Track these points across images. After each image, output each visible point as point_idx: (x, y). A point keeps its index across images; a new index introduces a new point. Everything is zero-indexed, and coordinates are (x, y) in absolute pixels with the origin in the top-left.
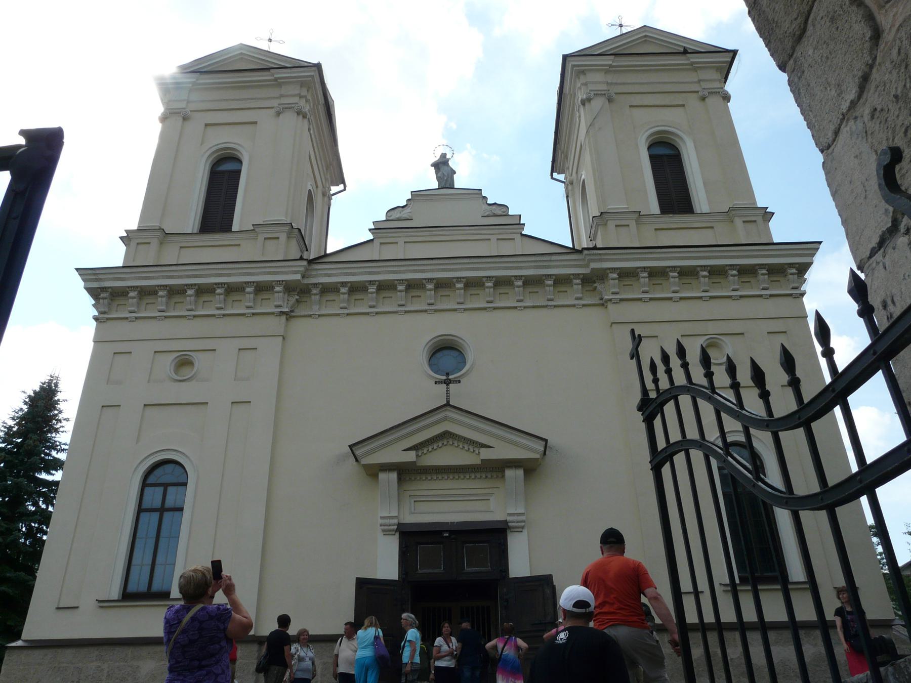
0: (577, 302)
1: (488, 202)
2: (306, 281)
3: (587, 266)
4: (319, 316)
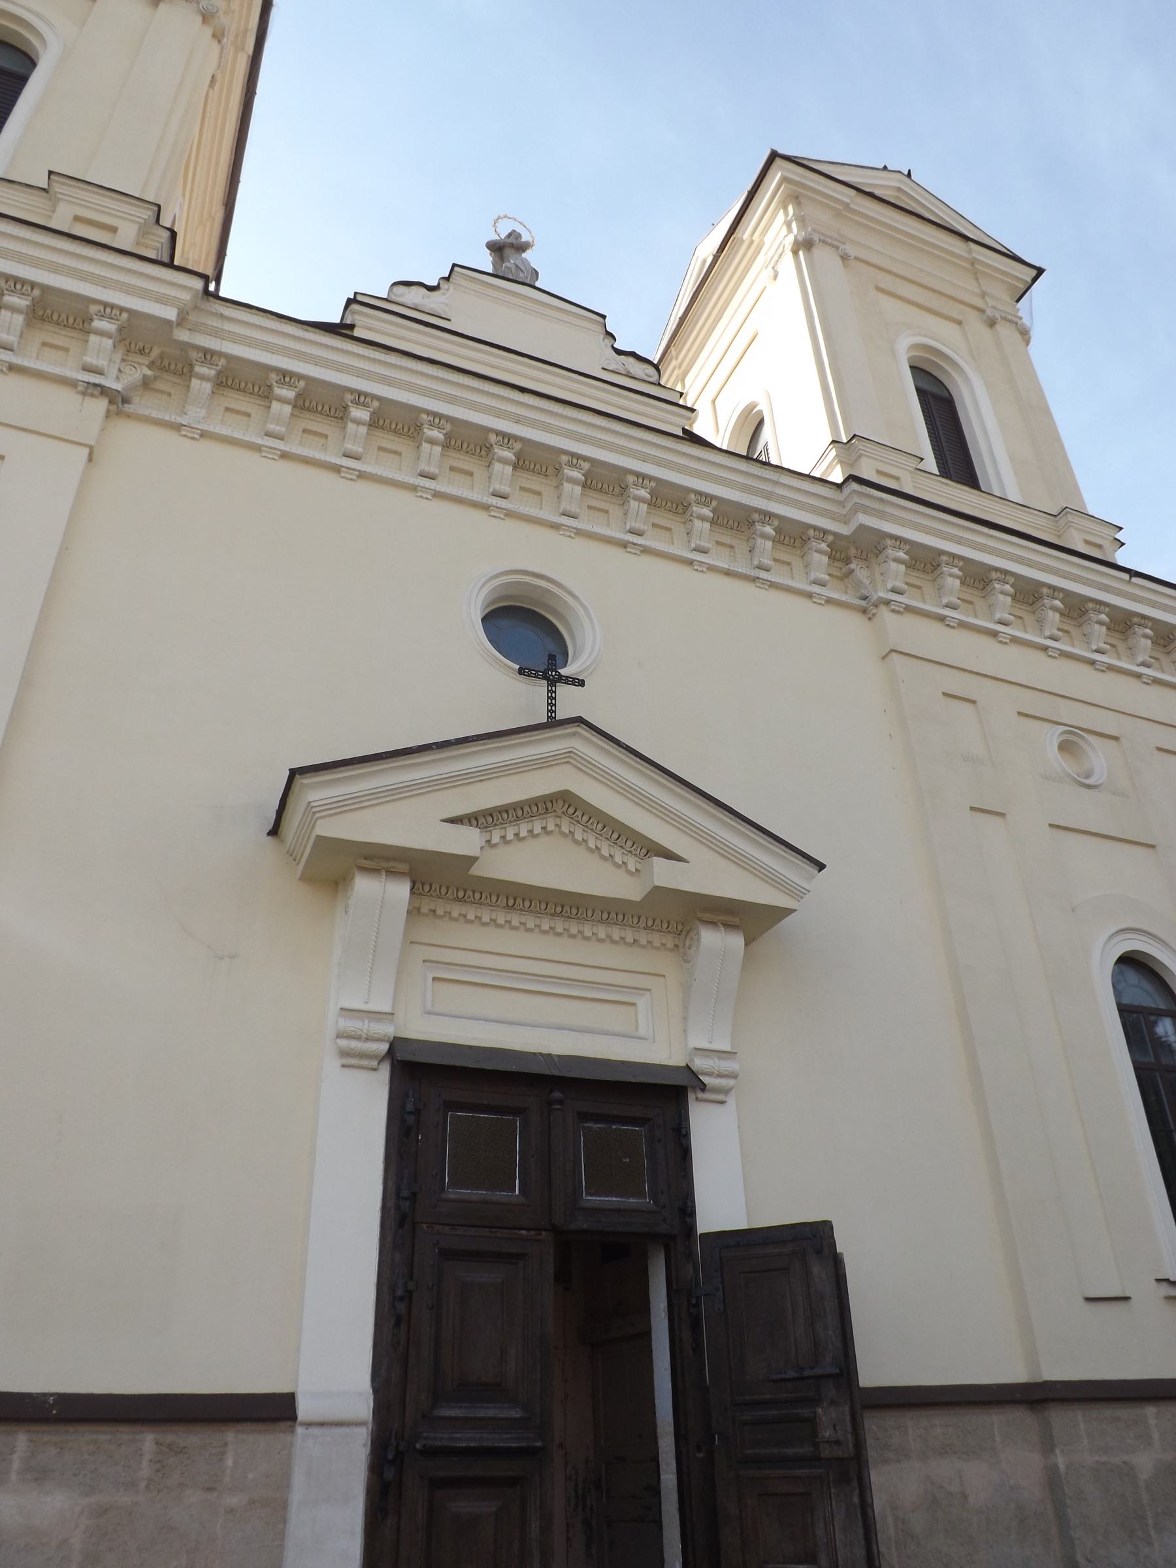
0: (815, 589)
1: (615, 346)
2: (183, 335)
3: (845, 520)
4: (204, 435)
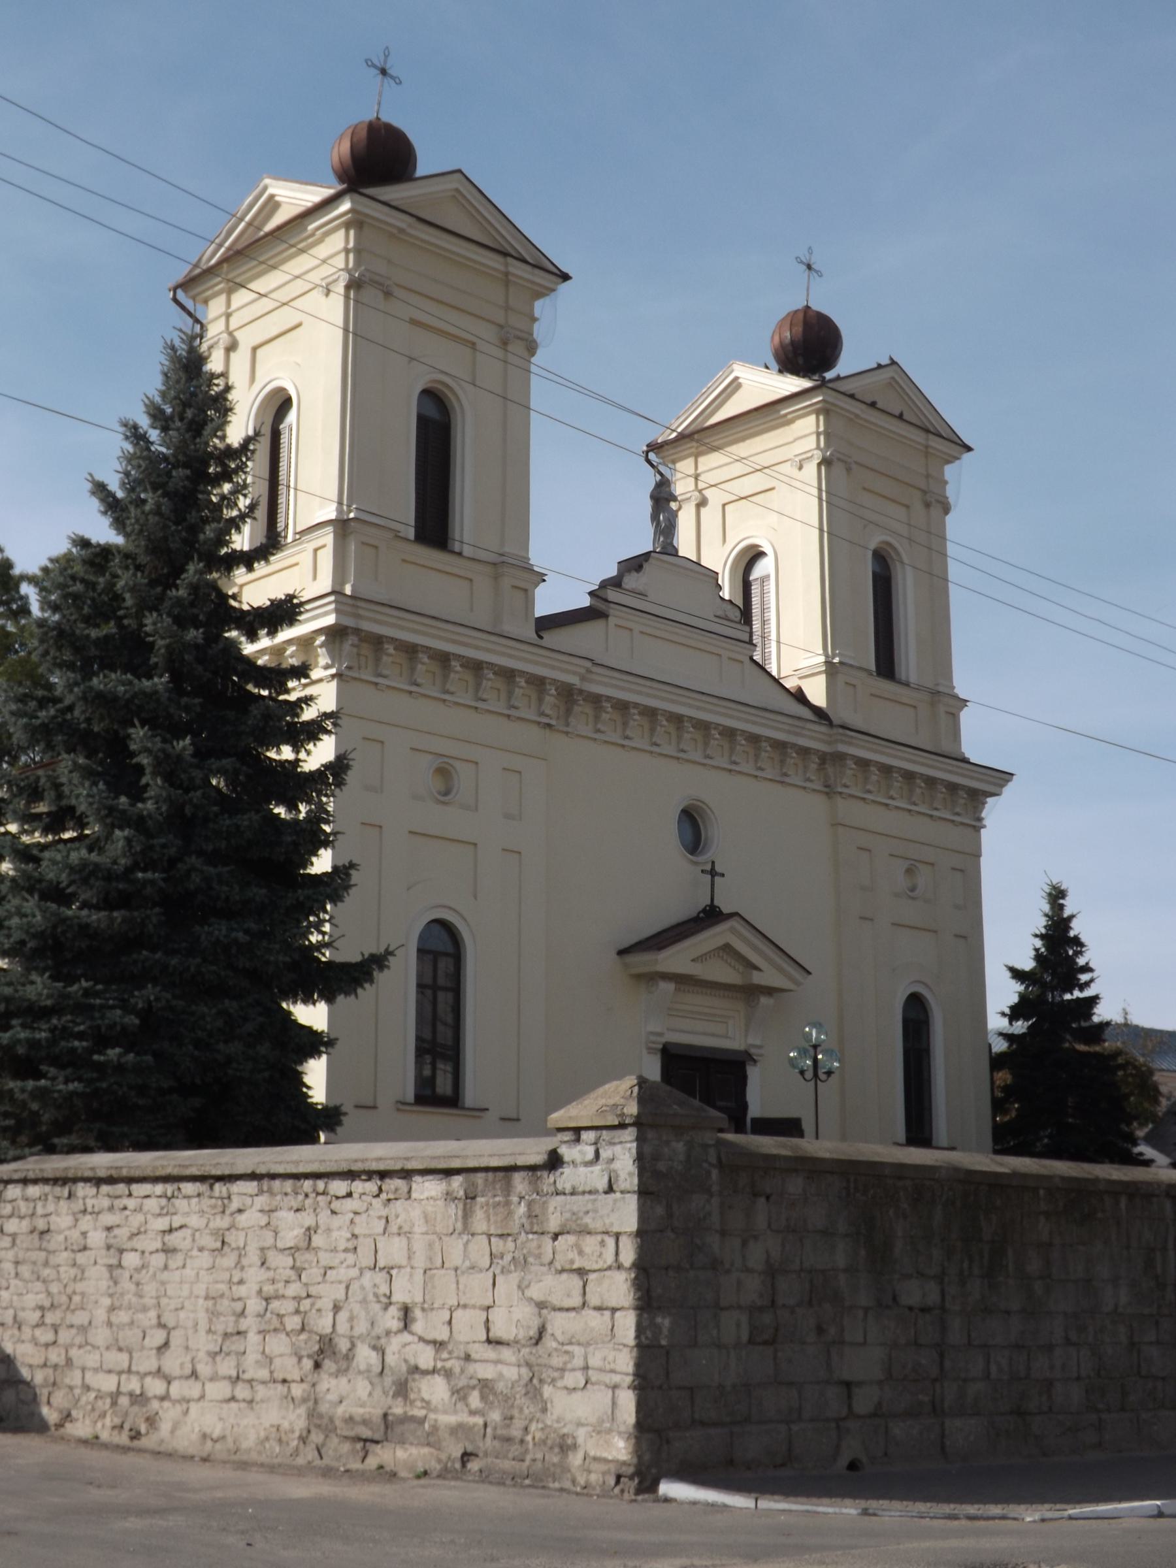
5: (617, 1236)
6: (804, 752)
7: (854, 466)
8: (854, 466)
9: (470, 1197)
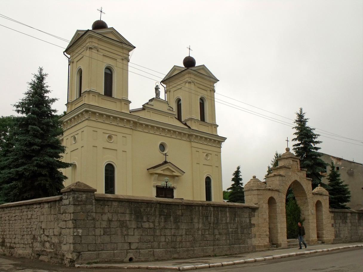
0: (186, 140)
3: (190, 132)
5: (71, 213)
6: (185, 134)
7: (195, 83)
8: (195, 83)
9: (51, 207)
